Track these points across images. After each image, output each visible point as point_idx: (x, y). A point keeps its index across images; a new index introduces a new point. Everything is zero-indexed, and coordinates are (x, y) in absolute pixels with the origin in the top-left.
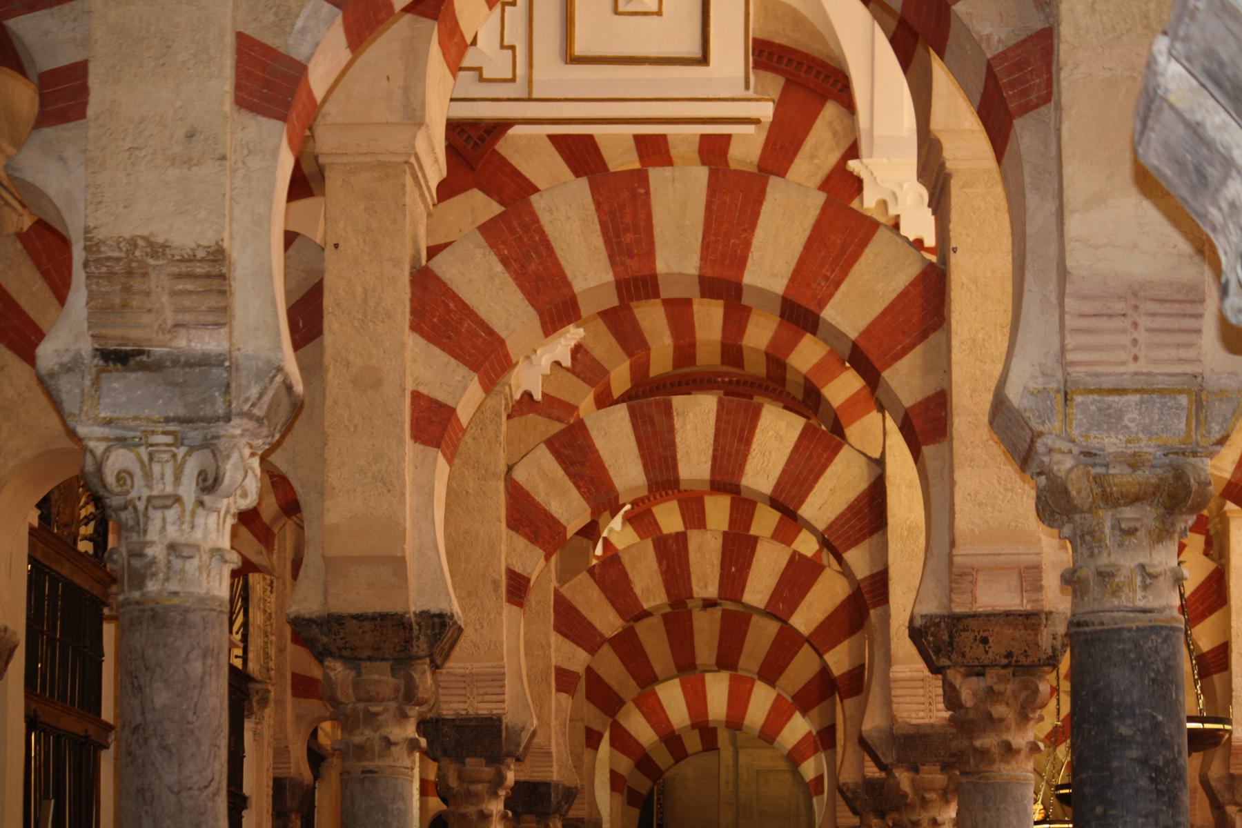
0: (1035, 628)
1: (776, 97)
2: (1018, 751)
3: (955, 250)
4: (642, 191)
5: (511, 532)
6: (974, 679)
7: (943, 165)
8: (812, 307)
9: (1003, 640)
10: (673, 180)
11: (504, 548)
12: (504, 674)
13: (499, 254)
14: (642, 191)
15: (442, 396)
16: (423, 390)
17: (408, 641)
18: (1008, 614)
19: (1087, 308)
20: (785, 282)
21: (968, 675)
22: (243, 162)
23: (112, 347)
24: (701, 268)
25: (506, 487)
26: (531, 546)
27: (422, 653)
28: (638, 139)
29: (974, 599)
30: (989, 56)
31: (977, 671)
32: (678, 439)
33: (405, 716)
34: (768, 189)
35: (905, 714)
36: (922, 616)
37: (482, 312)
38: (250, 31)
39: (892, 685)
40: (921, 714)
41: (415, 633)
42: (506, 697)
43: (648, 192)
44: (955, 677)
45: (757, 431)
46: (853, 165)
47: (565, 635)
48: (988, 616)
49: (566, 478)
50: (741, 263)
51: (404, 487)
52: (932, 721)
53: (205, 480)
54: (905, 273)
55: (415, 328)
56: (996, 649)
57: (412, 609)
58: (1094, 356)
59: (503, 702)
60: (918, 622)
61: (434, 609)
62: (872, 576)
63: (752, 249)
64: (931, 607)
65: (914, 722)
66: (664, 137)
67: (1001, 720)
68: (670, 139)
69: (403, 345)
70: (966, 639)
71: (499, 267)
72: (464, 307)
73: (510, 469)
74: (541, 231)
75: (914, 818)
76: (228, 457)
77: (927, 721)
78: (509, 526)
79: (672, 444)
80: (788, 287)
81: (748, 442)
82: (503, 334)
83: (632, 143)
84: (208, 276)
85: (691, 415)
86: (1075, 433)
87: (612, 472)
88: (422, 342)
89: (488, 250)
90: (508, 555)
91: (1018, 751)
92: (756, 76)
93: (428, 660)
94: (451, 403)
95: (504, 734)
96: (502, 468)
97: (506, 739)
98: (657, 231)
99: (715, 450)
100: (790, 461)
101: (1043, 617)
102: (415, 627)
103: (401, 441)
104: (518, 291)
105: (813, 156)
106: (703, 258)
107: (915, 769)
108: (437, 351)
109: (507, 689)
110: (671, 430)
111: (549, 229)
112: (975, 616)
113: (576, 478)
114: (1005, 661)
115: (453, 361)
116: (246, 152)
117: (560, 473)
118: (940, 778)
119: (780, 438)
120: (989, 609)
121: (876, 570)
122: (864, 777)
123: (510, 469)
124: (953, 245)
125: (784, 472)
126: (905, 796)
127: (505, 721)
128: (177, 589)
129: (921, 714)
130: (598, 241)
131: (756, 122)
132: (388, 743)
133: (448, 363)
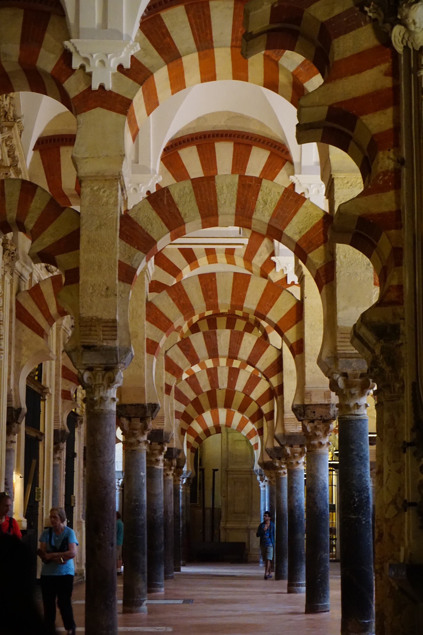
0: (329, 409)
1: (249, 236)
2: (324, 445)
3: (306, 298)
4: (214, 279)
5: (166, 372)
6: (311, 424)
7: (302, 272)
8: (264, 314)
9: (319, 412)
10: (223, 276)
11: (164, 377)
12: (164, 416)
13: (171, 297)
14: (214, 279)
15: (155, 340)
16: (150, 338)
17: (145, 412)
18: (321, 405)
19: (343, 336)
20: (256, 306)
22: (121, 295)
23: (86, 344)
24: (231, 302)
25: (165, 358)
26: (173, 376)
27: (149, 415)
28: (206, 249)
29: (311, 400)
30: (317, 268)
31: (312, 421)
32: (218, 343)
33: (144, 434)
34: (251, 279)
35: (289, 429)
36: (296, 405)
37: (167, 315)
38: (122, 260)
39: (285, 420)
40: (294, 429)
41: (147, 410)
42: (165, 423)
43: (215, 279)
44: (306, 424)
45: (243, 340)
46: (273, 258)
47: (178, 400)
48: (316, 405)
49: (184, 355)
50: (243, 301)
51: (144, 366)
52: (297, 431)
53: (111, 380)
54: (291, 304)
55: (147, 319)
56: (317, 415)
57: (147, 402)
58: (344, 348)
59: (164, 425)
60: (295, 407)
61: (153, 403)
62: (278, 386)
63: (246, 296)
64: (298, 402)
65: (291, 431)
66: (214, 249)
67: (319, 436)
68: (216, 249)
69: (144, 325)
70: (309, 412)
71: (172, 302)
72: (162, 314)
73: (166, 352)
74: (185, 291)
75: (291, 461)
76: (117, 374)
77: (295, 431)
78: (166, 370)
79: (216, 345)
80: (257, 308)
81: (240, 344)
82: (173, 321)
83: (204, 251)
84: (112, 327)
85: (222, 336)
86: (339, 368)
87: (198, 353)
88: (149, 323)
89: (169, 296)
90: (166, 379)
91: (324, 445)
92: (243, 229)
93: (151, 417)
94: (158, 342)
95: (164, 435)
96: (164, 352)
97: (165, 436)
98: (218, 291)
99: (230, 346)
100: (253, 350)
101: (331, 405)
102: (147, 408)
103: (143, 353)
104: (178, 309)
105: (260, 255)
106: (232, 299)
107: (291, 446)
108: (153, 326)
109: (165, 421)
110: (216, 340)
111: (186, 290)
113: (187, 355)
114: (320, 418)
115: (159, 329)
116: (121, 293)
117: (181, 353)
118: (299, 450)
119: (250, 343)
120: (315, 403)
121: (279, 384)
122: (274, 446)
123: (166, 352)
124: (305, 296)
125: (251, 353)
126: (288, 455)
127: (164, 431)
128: (103, 408)
129: (294, 429)
130: (201, 294)
131: (243, 244)
132: (139, 442)
133: (157, 330)
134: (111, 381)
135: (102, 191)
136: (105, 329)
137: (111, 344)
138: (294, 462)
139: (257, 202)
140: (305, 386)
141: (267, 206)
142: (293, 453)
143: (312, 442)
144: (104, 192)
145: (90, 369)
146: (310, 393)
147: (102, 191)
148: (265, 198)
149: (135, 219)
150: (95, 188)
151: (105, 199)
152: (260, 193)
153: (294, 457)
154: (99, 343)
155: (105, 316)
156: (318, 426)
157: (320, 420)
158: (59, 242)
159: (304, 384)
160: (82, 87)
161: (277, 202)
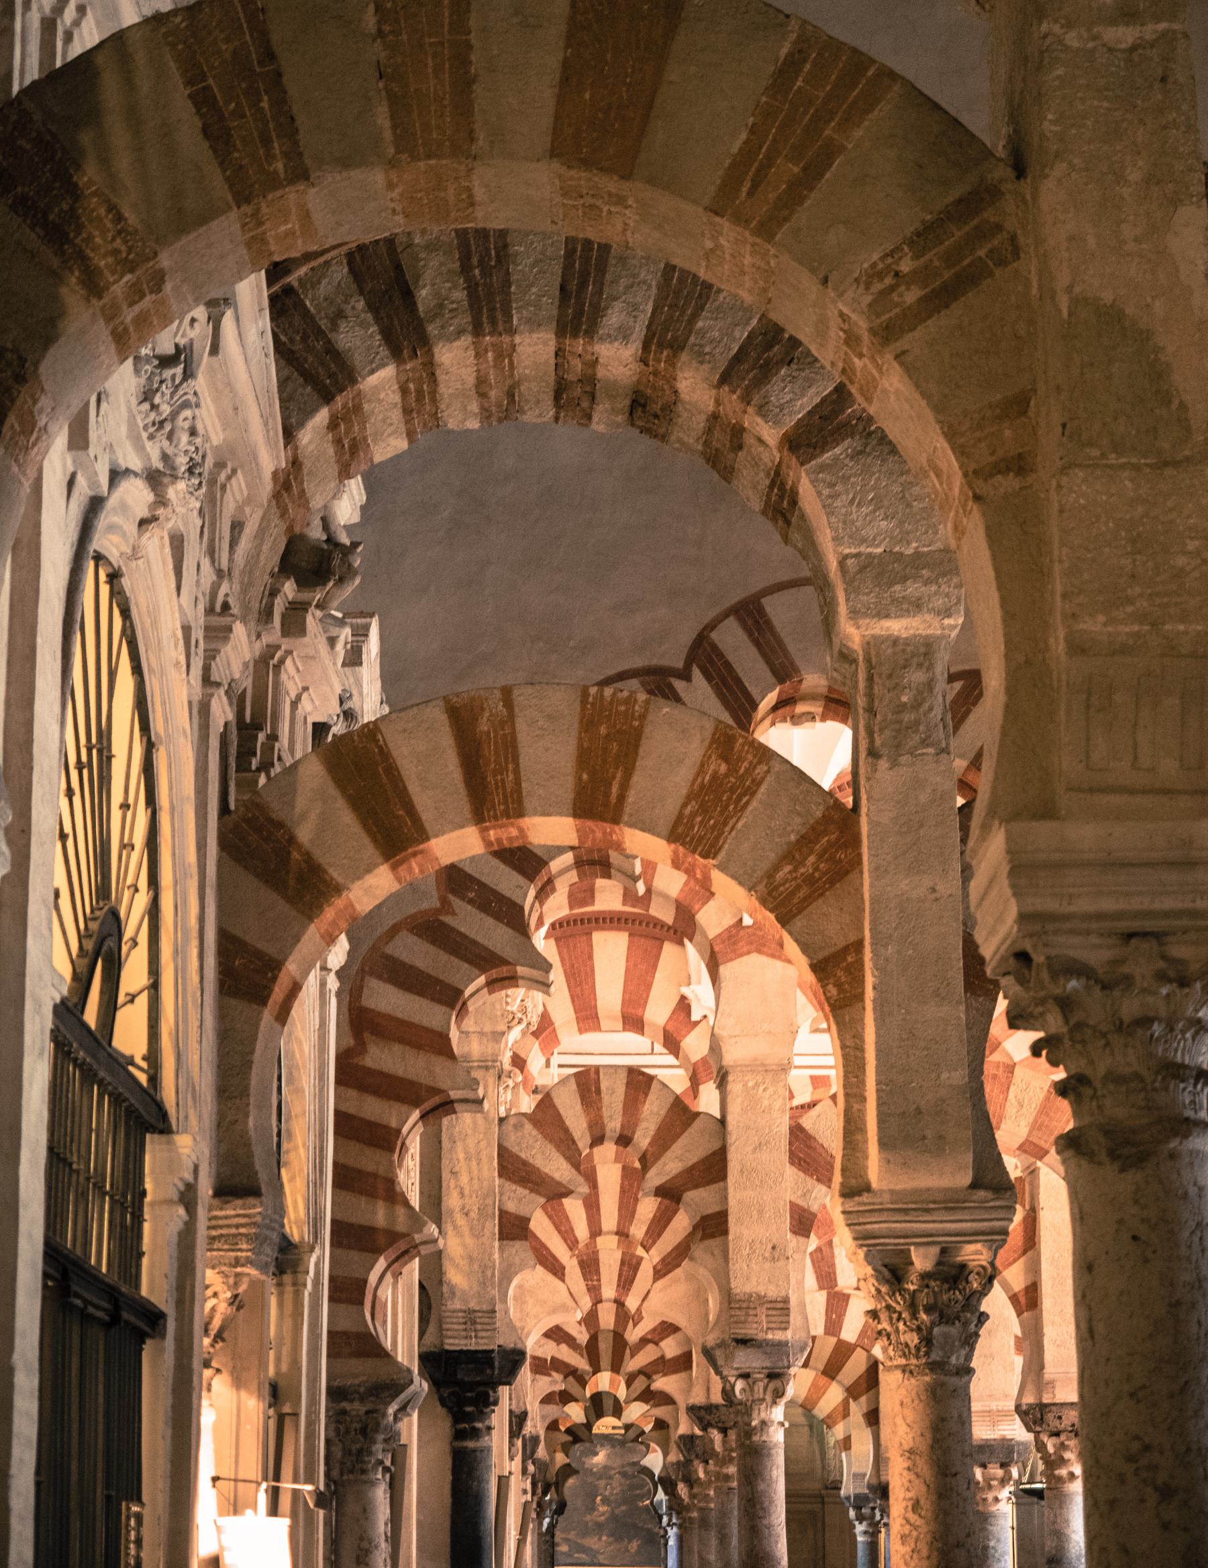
23: (740, 1337)
28: (813, 1078)
29: (1054, 1396)
32: (837, 1262)
38: (793, 1199)
44: (1044, 1438)
48: (1062, 1405)
52: (995, 1437)
70: (1050, 1417)
77: (992, 1437)
83: (809, 1081)
107: (984, 1466)
118: (1000, 1473)
126: (978, 1483)
134: (779, 1394)
135: (761, 1088)
136: (770, 1312)
137: (778, 1336)
139: (1008, 1104)
141: (1024, 1110)
143: (1057, 1472)
144: (765, 1090)
145: (745, 1376)
146: (1052, 1383)
147: (761, 1088)
148: (1020, 1097)
149: (811, 1132)
150: (750, 1084)
151: (766, 1103)
152: (1012, 1088)
153: (990, 1487)
154: (761, 1336)
155: (772, 1292)
158: (690, 1170)
159: (1042, 1367)
160: (729, 921)
161: (1039, 1103)
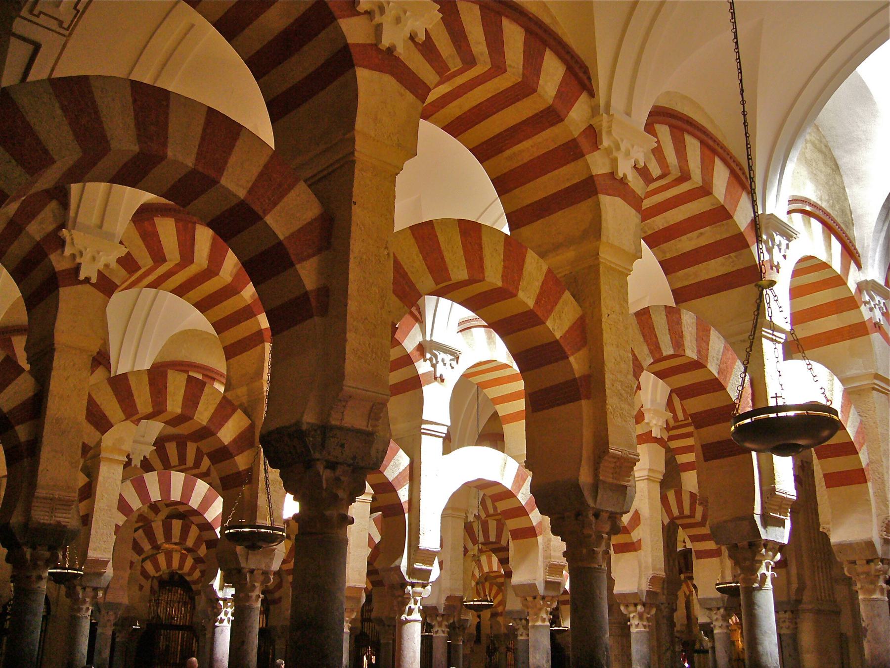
7: (353, 153)
21: (326, 467)
35: (37, 517)
36: (308, 423)
107: (34, 548)
112: (340, 428)
138: (34, 574)
140: (344, 383)
142: (34, 559)
156: (342, 478)
157: (349, 465)
